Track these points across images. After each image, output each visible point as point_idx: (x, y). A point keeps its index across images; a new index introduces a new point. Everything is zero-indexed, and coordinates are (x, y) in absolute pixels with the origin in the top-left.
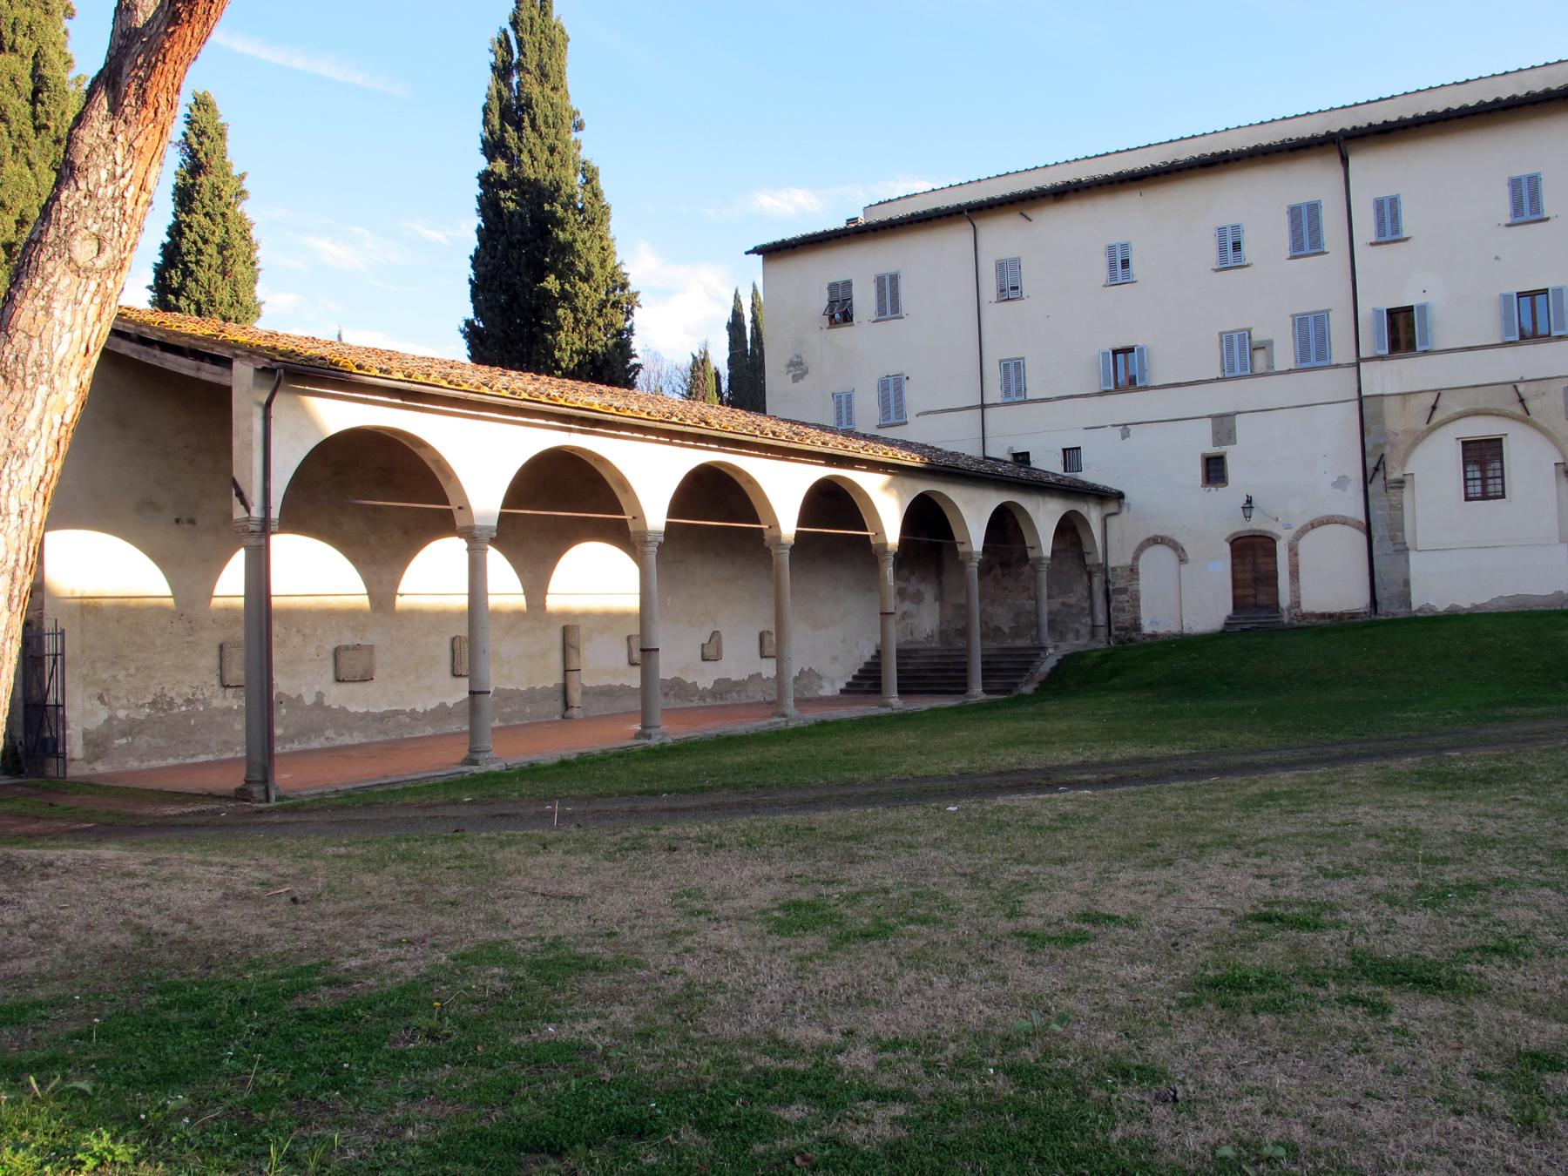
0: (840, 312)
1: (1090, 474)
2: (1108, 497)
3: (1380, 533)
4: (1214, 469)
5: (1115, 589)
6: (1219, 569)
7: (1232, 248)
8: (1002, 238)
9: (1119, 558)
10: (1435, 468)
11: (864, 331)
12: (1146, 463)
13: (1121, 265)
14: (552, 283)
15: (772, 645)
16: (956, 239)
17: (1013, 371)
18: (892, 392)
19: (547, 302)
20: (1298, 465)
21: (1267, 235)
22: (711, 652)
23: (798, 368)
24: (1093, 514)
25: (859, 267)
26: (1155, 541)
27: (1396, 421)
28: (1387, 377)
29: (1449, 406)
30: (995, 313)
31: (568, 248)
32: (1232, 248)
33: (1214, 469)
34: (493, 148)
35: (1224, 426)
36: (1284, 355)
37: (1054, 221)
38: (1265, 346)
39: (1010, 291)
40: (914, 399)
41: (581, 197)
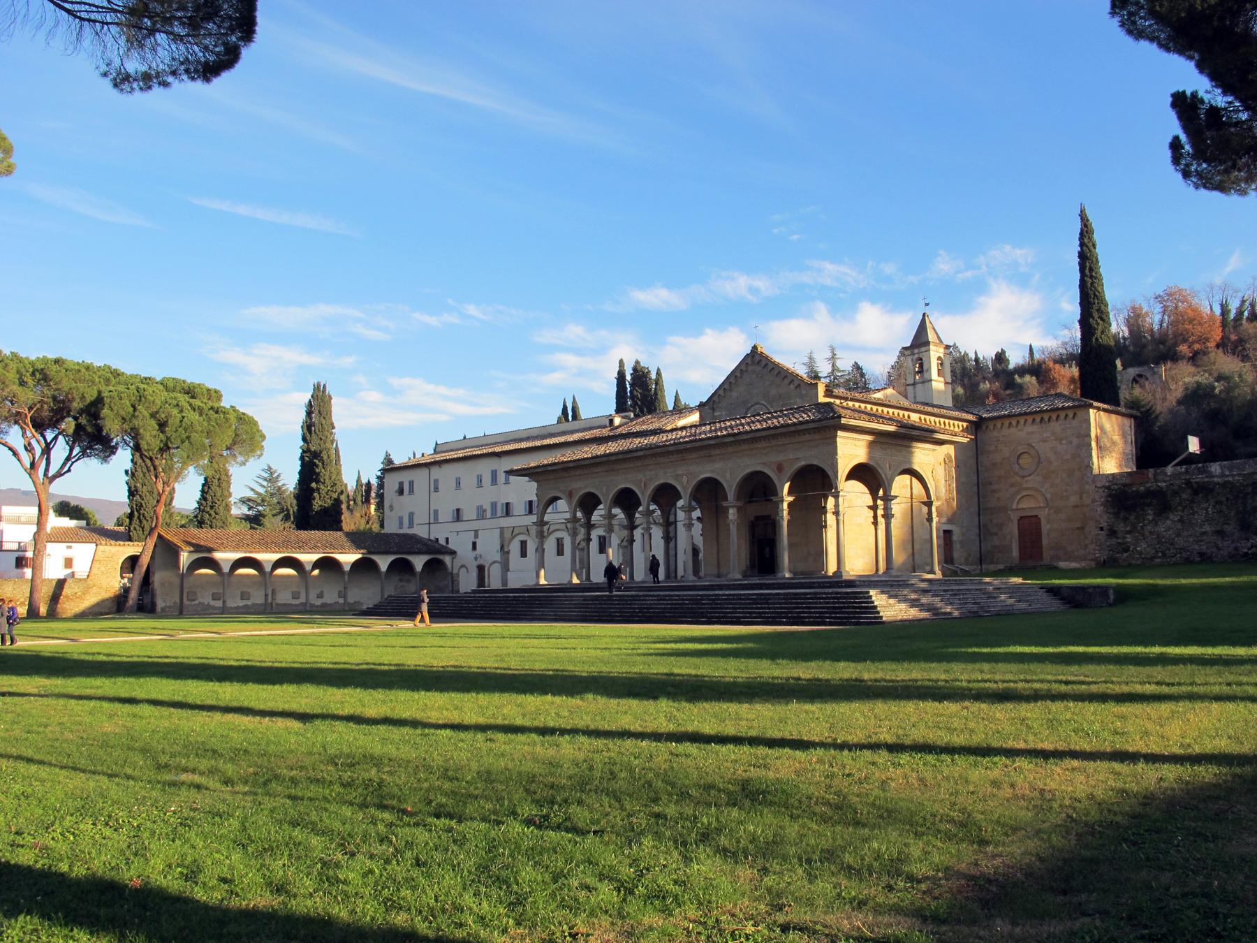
0: (401, 492)
1: (451, 546)
2: (453, 553)
3: (505, 568)
4: (474, 545)
5: (454, 579)
6: (474, 574)
7: (480, 480)
8: (436, 472)
9: (455, 571)
10: (515, 547)
11: (406, 497)
12: (460, 543)
13: (458, 483)
14: (314, 485)
15: (343, 595)
16: (425, 471)
17: (436, 512)
18: (411, 515)
19: (313, 490)
20: (489, 548)
21: (487, 479)
22: (320, 596)
23: (391, 508)
24: (447, 559)
25: (405, 477)
26: (463, 566)
27: (507, 535)
28: (507, 522)
29: (516, 531)
30: (433, 494)
31: (318, 474)
32: (480, 480)
33: (474, 545)
34: (304, 439)
35: (476, 532)
36: (489, 515)
37: (447, 469)
38: (485, 511)
39: (436, 489)
40: (416, 521)
41: (325, 457)
